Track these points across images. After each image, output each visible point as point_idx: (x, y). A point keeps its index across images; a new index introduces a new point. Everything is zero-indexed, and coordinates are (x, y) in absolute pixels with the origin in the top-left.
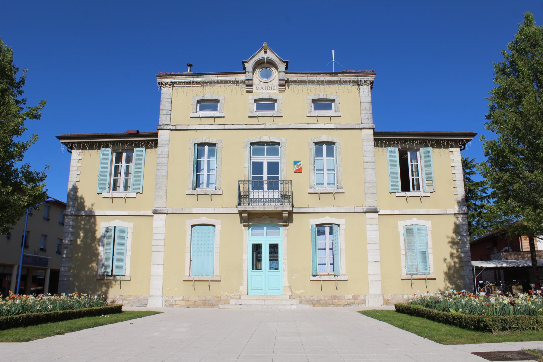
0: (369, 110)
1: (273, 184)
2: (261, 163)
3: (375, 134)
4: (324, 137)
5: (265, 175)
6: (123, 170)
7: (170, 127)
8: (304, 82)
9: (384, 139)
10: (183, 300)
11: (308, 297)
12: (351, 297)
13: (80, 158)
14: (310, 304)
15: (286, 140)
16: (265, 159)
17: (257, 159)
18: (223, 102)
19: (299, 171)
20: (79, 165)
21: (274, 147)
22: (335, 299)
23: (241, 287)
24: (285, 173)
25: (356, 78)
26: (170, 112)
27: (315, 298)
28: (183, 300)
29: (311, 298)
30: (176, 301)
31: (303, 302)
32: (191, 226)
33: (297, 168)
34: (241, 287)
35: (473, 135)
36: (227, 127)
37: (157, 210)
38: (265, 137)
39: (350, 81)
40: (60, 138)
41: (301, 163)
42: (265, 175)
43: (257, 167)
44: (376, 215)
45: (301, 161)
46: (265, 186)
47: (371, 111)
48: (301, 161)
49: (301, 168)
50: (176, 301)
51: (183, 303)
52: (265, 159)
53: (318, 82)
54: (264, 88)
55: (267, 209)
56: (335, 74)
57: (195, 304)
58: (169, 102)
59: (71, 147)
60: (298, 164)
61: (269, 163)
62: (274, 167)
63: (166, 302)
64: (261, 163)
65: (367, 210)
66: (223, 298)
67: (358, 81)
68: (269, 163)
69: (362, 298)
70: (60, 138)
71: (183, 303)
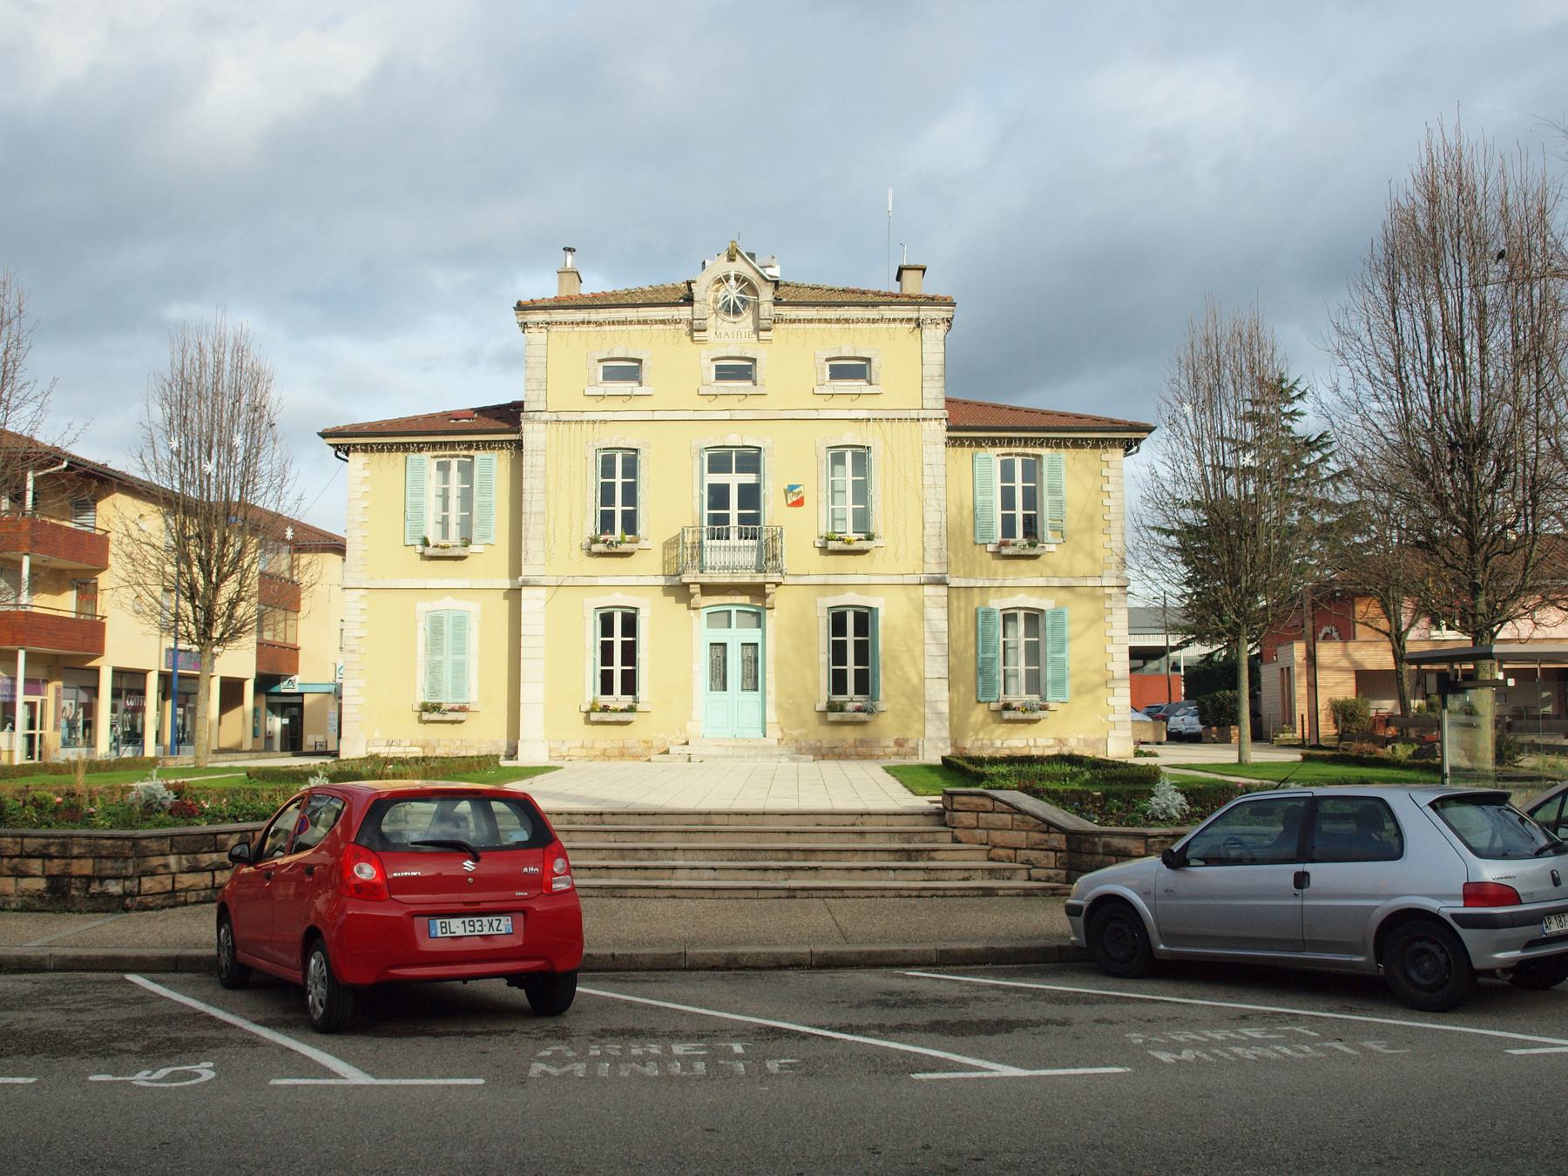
0: (938, 381)
1: (751, 524)
2: (725, 489)
3: (949, 429)
4: (851, 435)
5: (734, 511)
6: (454, 503)
7: (546, 416)
8: (810, 321)
9: (967, 438)
10: (582, 747)
11: (812, 742)
12: (892, 744)
13: (367, 473)
14: (815, 755)
15: (774, 442)
16: (734, 480)
17: (719, 479)
18: (649, 364)
19: (799, 503)
20: (366, 488)
21: (750, 460)
22: (862, 746)
23: (689, 723)
24: (773, 508)
25: (914, 315)
26: (544, 384)
27: (825, 744)
28: (582, 747)
29: (818, 744)
30: (569, 749)
31: (804, 751)
32: (593, 610)
33: (794, 499)
34: (689, 723)
35: (1150, 430)
36: (657, 416)
37: (529, 581)
38: (735, 437)
39: (902, 320)
40: (324, 435)
41: (801, 488)
42: (734, 511)
43: (718, 496)
44: (942, 590)
45: (798, 486)
46: (734, 535)
47: (941, 384)
48: (798, 486)
49: (802, 498)
50: (569, 749)
51: (583, 752)
52: (734, 480)
53: (838, 321)
54: (730, 335)
55: (735, 580)
56: (873, 306)
57: (605, 756)
58: (540, 363)
59: (344, 451)
60: (796, 491)
61: (743, 489)
62: (750, 496)
63: (550, 751)
64: (725, 489)
65: (927, 581)
66: (655, 744)
67: (918, 319)
68: (743, 489)
69: (912, 744)
70: (324, 435)
71: (583, 752)
